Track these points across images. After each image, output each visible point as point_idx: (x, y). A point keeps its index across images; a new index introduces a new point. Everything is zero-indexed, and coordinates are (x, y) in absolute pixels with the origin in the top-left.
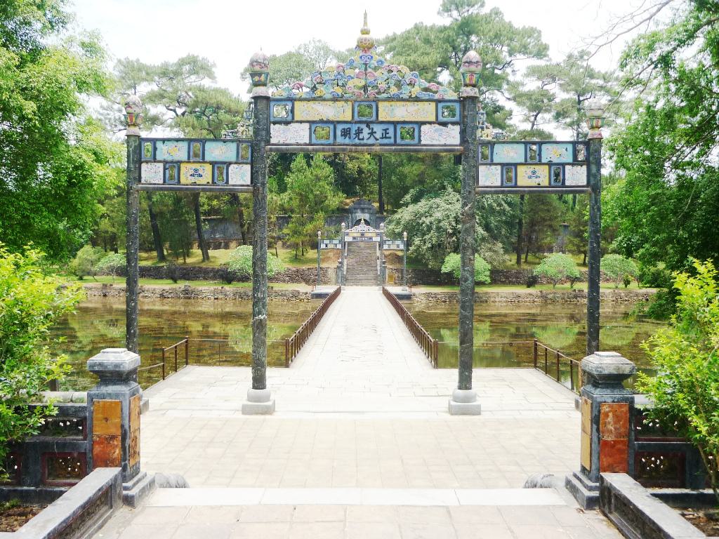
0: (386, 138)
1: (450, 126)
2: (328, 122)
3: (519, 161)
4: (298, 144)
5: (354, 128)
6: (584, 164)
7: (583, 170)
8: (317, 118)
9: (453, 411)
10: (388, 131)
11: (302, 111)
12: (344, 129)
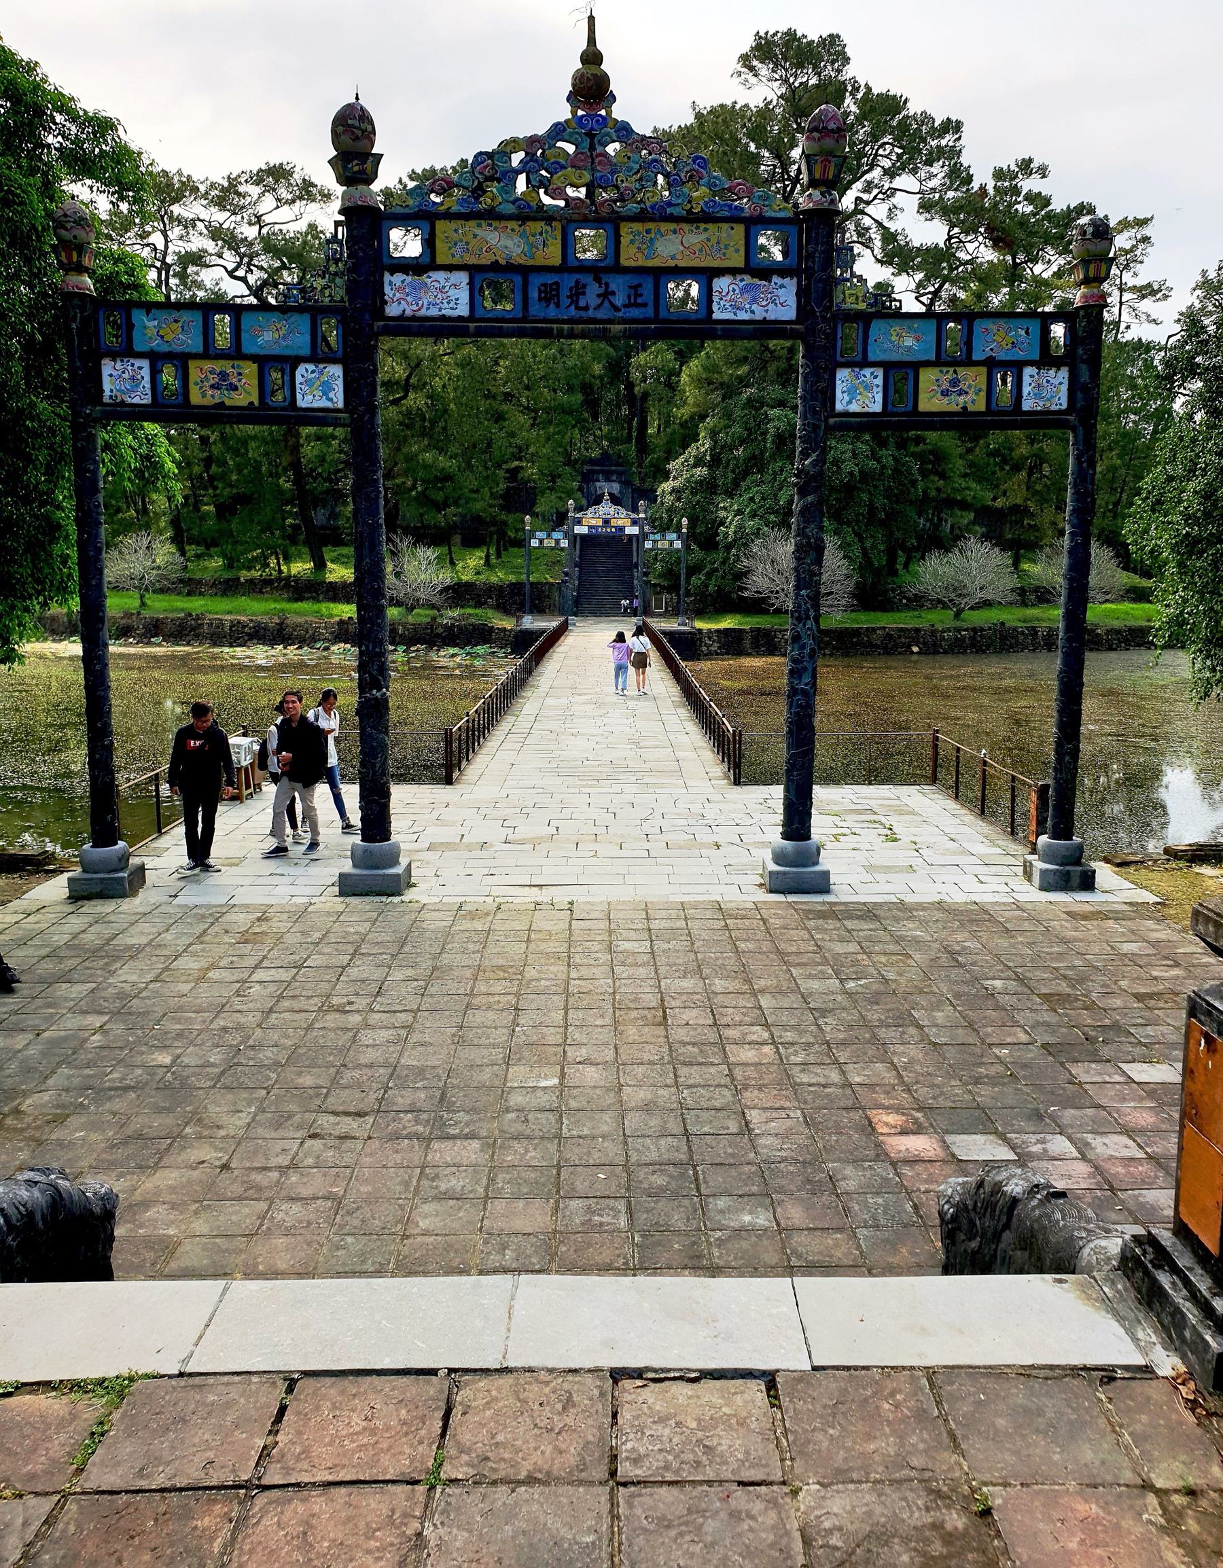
0: (636, 305)
1: (775, 279)
3: (924, 358)
4: (443, 318)
5: (568, 281)
6: (1065, 365)
7: (1059, 379)
8: (486, 259)
9: (778, 885)
10: (640, 291)
12: (545, 285)
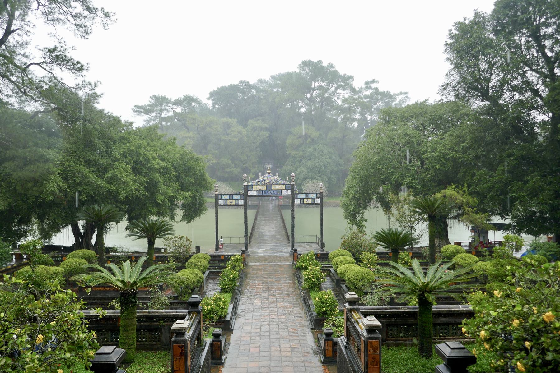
5: (267, 191)
11: (255, 188)
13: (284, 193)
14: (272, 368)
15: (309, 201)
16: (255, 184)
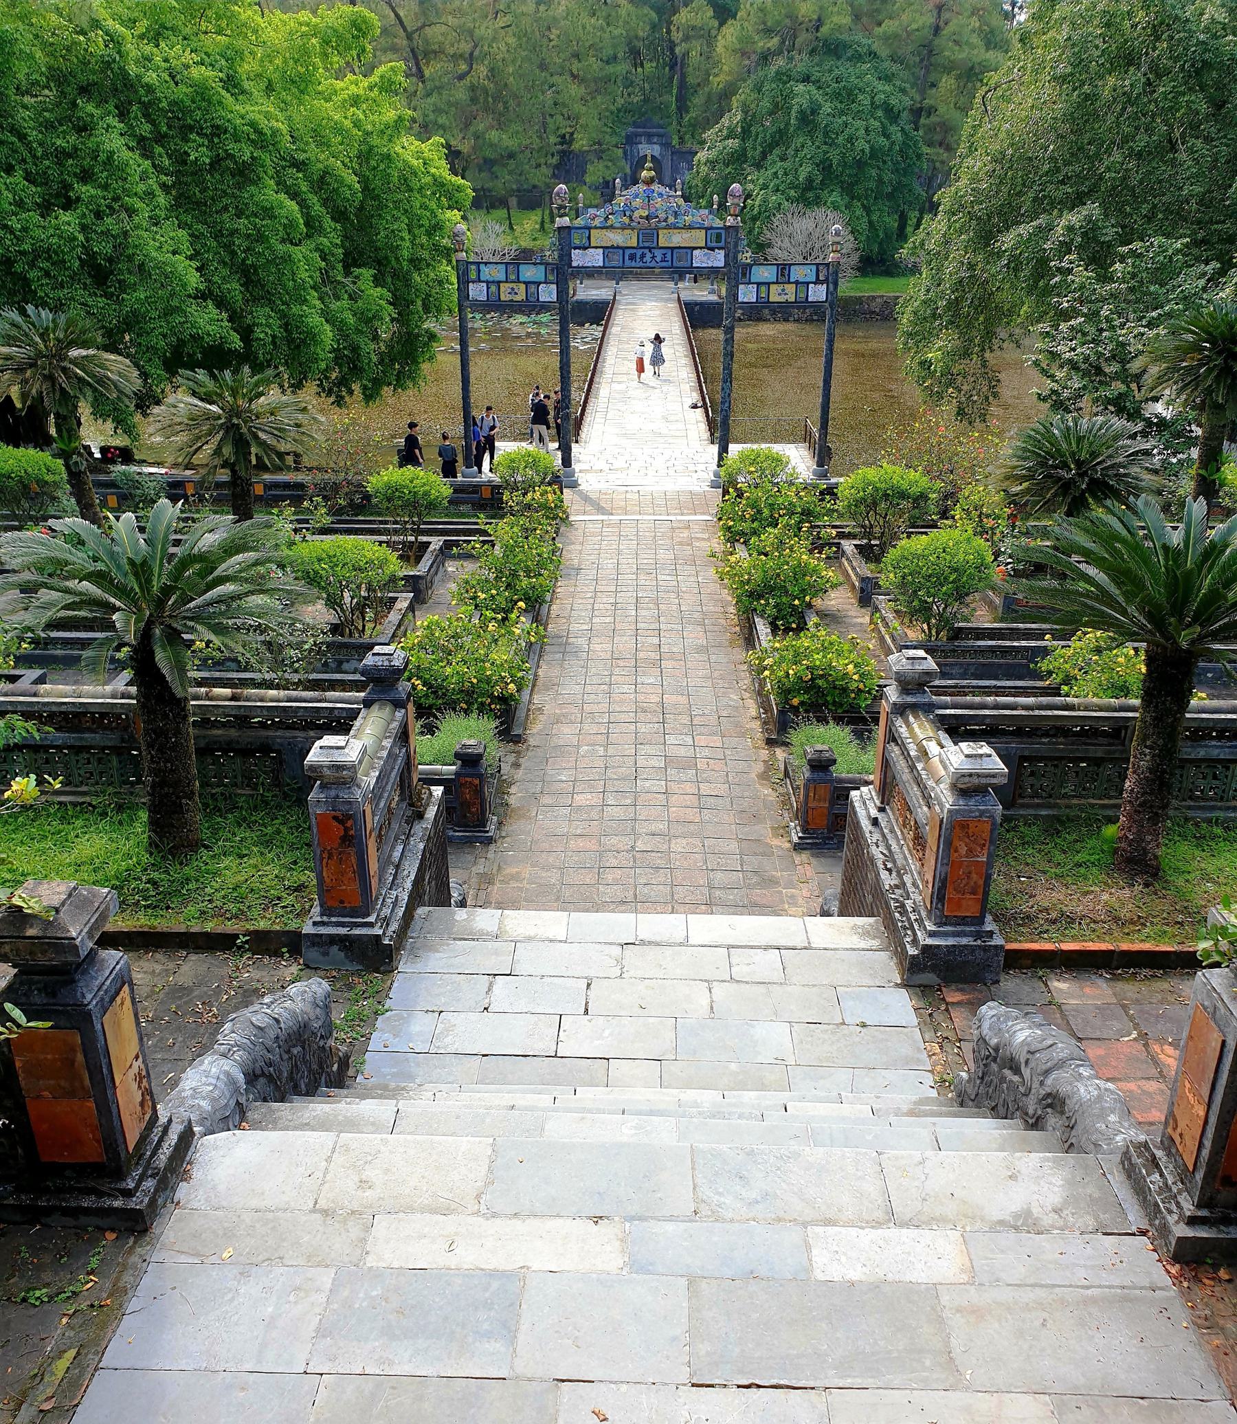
2: (618, 247)
5: (639, 252)
11: (598, 237)
13: (700, 259)
14: (638, 855)
15: (790, 294)
16: (597, 222)
